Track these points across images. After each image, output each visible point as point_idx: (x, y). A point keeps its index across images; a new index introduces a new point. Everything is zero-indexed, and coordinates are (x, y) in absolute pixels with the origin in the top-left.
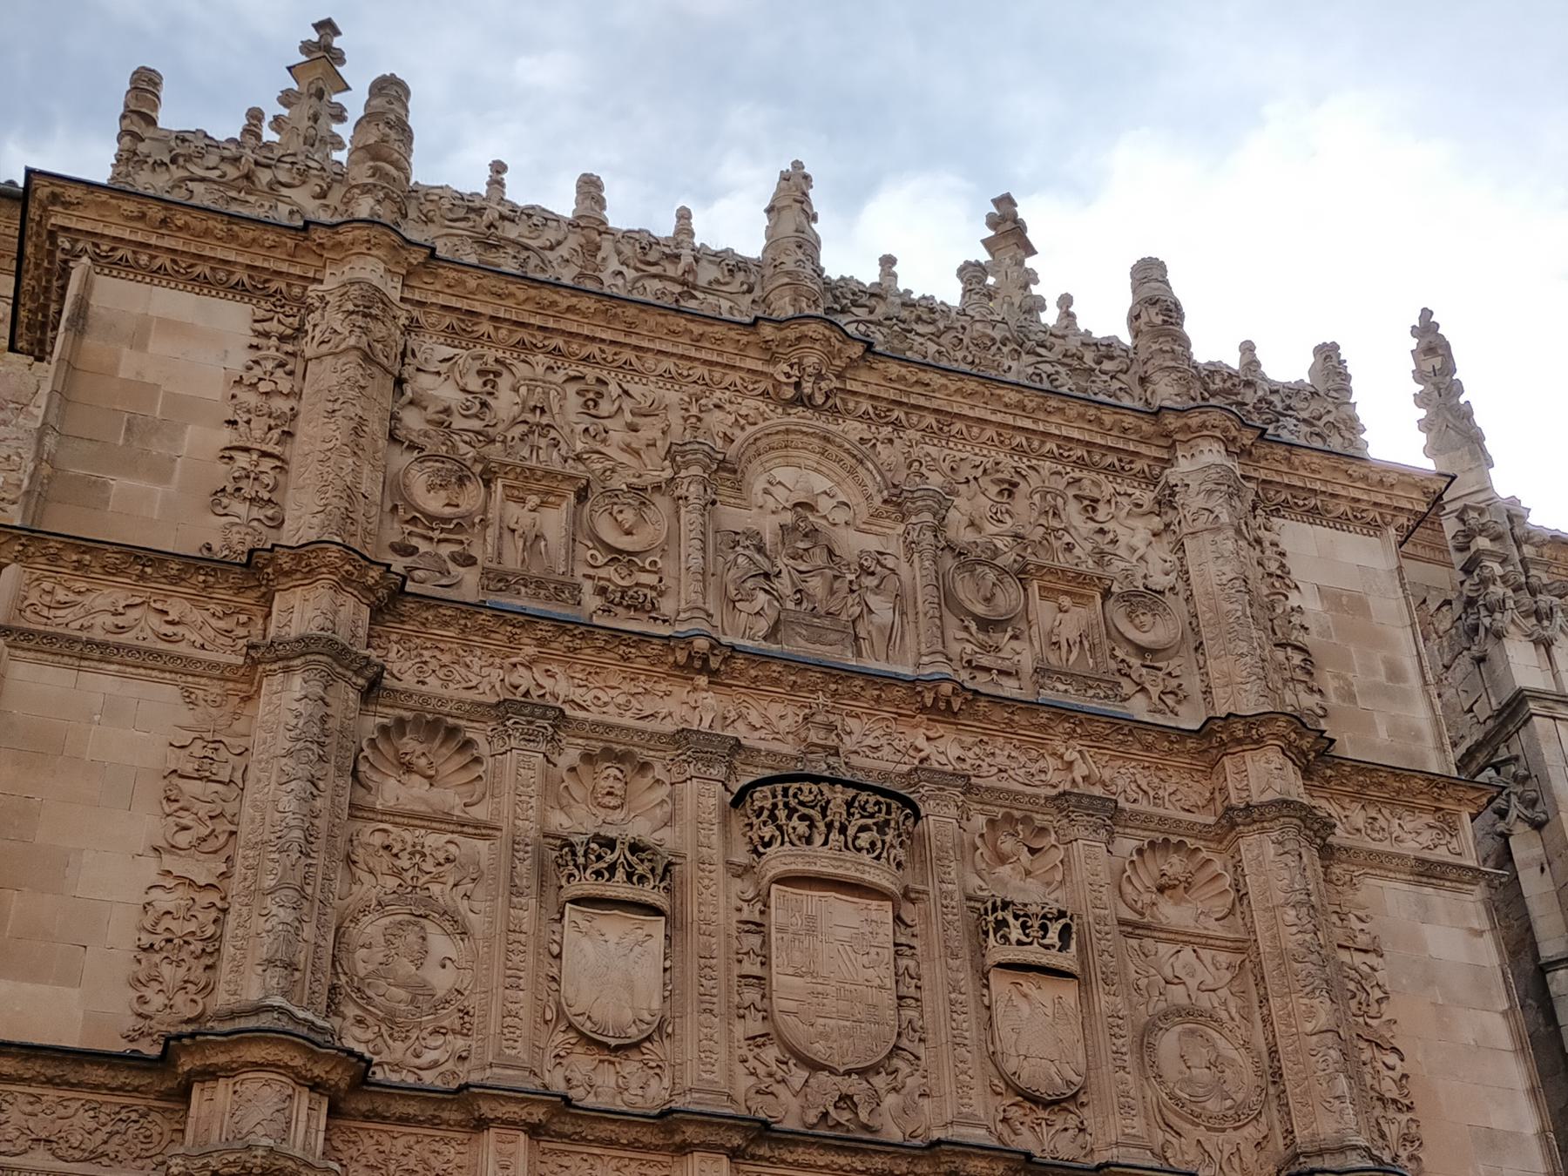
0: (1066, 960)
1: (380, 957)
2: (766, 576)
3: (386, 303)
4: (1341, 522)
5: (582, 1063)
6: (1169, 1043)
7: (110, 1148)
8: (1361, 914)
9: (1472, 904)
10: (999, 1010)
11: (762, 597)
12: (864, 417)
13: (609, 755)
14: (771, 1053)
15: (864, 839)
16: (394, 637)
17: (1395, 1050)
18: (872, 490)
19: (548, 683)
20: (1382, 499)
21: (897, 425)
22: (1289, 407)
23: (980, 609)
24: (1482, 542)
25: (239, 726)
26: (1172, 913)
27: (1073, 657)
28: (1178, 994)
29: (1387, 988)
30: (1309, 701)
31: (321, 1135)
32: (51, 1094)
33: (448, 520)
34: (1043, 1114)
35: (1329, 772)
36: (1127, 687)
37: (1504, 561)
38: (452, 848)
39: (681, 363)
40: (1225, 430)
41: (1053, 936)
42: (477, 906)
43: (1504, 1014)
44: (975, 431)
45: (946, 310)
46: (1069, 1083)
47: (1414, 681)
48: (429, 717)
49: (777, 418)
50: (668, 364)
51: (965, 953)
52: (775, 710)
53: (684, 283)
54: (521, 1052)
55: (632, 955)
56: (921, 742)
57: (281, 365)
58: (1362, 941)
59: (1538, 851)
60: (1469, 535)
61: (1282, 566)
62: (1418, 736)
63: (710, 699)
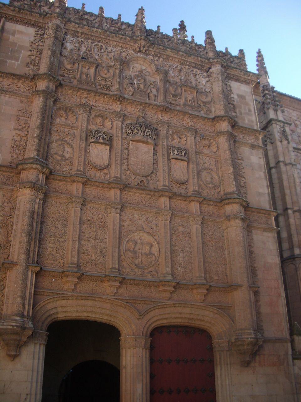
0: (186, 159)
1: (55, 151)
2: (132, 84)
3: (61, 28)
6: (204, 174)
8: (240, 153)
9: (260, 153)
11: (131, 88)
12: (153, 56)
14: (128, 173)
15: (148, 134)
16: (60, 92)
17: (244, 177)
18: (153, 69)
19: (89, 102)
20: (249, 78)
21: (159, 58)
22: (234, 60)
23: (173, 93)
24: (266, 92)
25: (30, 107)
26: (205, 151)
27: (190, 103)
28: (206, 166)
29: (244, 166)
30: (234, 114)
31: (44, 182)
33: (70, 70)
34: (179, 185)
35: (236, 127)
37: (270, 95)
39: (118, 43)
40: (221, 63)
41: (183, 154)
42: (74, 142)
43: (264, 172)
44: (174, 59)
45: (170, 37)
46: (185, 180)
47: (253, 112)
49: (136, 55)
50: (114, 43)
51: (166, 156)
53: (119, 28)
54: (82, 169)
55: (103, 153)
56: (160, 117)
57: (40, 40)
58: (240, 158)
59: (271, 148)
60: (264, 90)
61: (230, 89)
62: (253, 122)
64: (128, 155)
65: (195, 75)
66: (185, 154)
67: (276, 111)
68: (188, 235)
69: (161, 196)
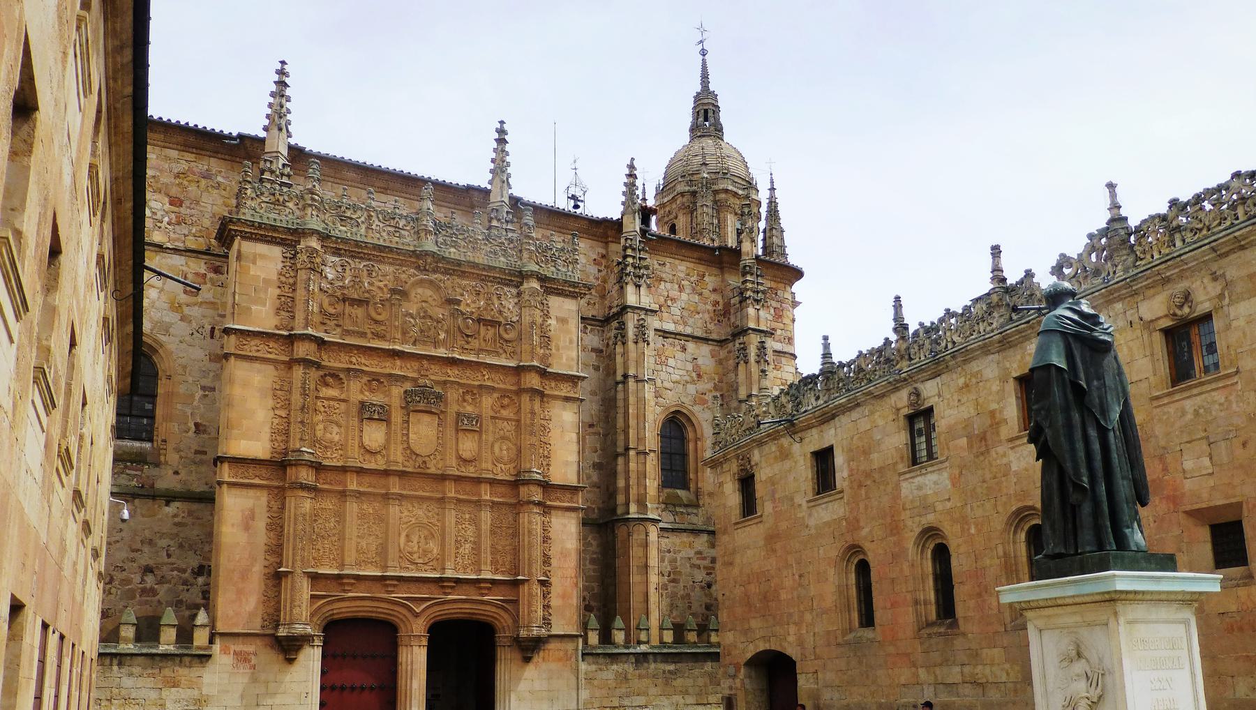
4: (566, 296)
5: (367, 457)
7: (271, 477)
10: (460, 439)
12: (442, 273)
13: (374, 380)
19: (359, 359)
20: (577, 290)
21: (451, 274)
26: (505, 413)
32: (258, 466)
36: (501, 351)
37: (634, 257)
38: (338, 406)
41: (474, 423)
47: (575, 344)
48: (332, 372)
52: (413, 364)
56: (449, 371)
62: (572, 359)
63: (398, 362)
64: (408, 431)
65: (499, 298)
66: (477, 421)
67: (638, 286)
68: (476, 522)
69: (445, 479)
